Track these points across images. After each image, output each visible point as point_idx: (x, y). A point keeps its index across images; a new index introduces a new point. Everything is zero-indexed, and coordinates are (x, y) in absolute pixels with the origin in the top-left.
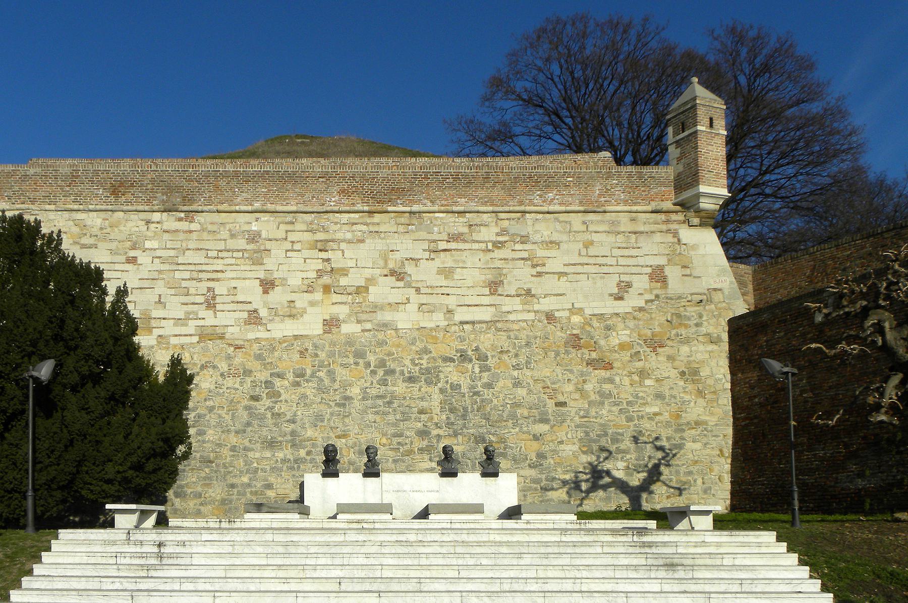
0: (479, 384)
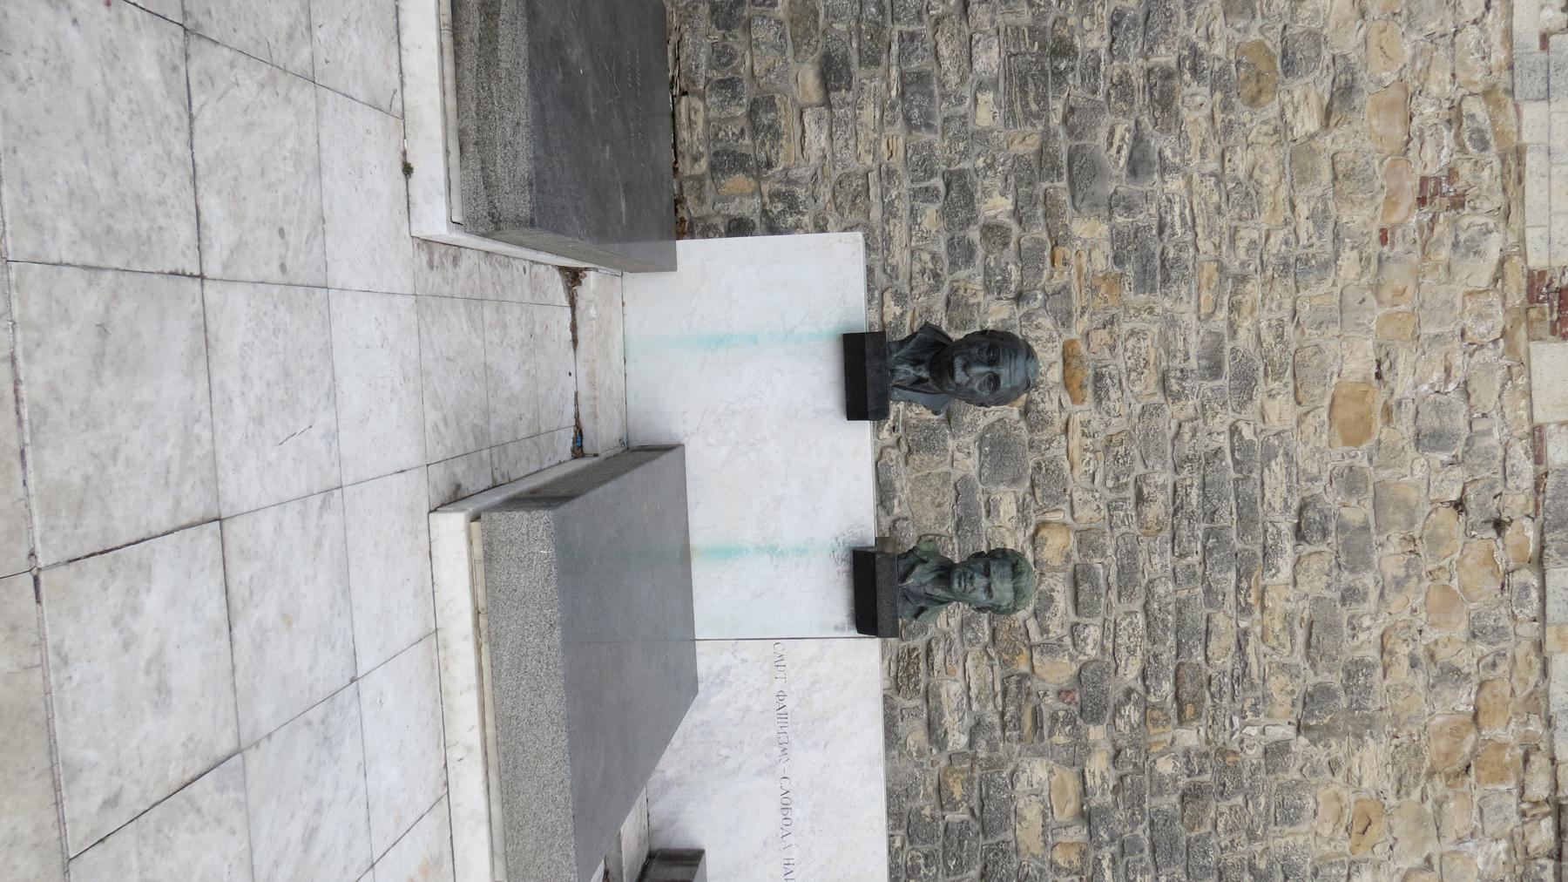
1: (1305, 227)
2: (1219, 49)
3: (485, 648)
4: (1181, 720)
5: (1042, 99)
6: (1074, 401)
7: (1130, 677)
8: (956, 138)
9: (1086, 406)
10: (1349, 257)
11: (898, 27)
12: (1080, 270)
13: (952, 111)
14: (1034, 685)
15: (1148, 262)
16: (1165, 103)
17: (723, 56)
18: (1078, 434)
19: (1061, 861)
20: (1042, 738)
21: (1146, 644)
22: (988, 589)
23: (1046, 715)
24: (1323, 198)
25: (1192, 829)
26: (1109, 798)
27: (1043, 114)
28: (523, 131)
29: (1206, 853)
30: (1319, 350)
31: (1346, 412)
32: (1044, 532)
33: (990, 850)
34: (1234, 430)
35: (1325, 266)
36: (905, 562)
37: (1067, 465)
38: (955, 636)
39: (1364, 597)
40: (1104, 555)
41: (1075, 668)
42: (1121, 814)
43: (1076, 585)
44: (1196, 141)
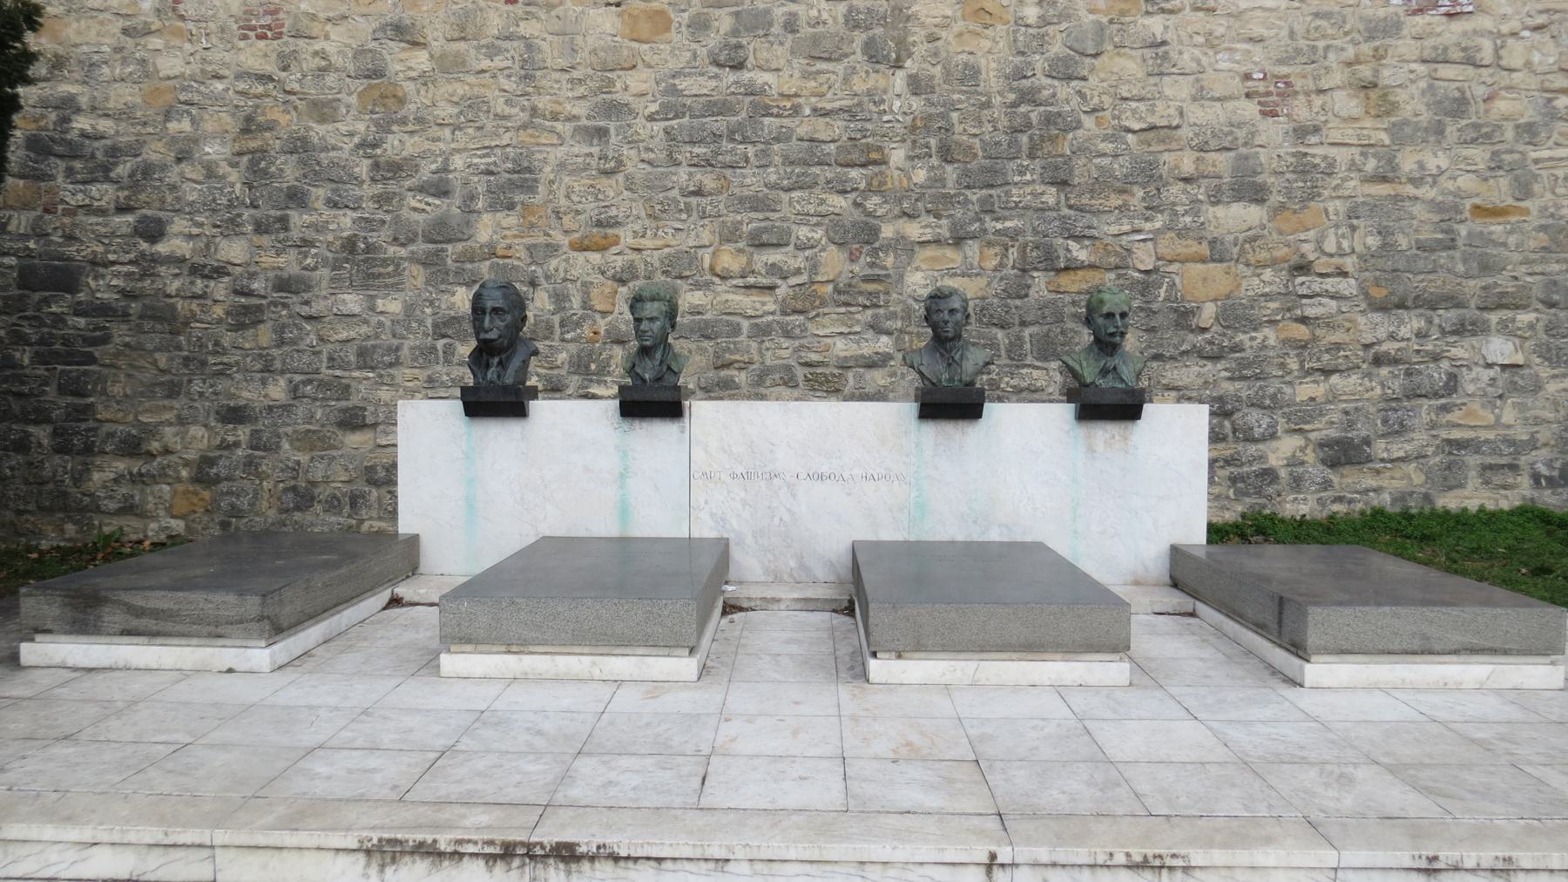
0: (1039, 62)
1: (499, 62)
2: (361, 127)
3: (532, 649)
4: (885, 163)
5: (385, 262)
6: (617, 244)
7: (844, 203)
8: (408, 329)
9: (621, 234)
10: (525, 29)
11: (323, 370)
12: (515, 236)
13: (388, 331)
14: (843, 280)
15: (515, 183)
16: (396, 169)
17: (333, 504)
18: (643, 241)
19: (994, 263)
20: (888, 276)
21: (817, 190)
22: (651, 319)
23: (870, 272)
24: (479, 48)
25: (976, 155)
26: (944, 222)
27: (396, 262)
28: (210, 597)
29: (998, 143)
30: (594, 52)
31: (645, 28)
32: (718, 270)
33: (980, 321)
34: (651, 118)
35: (529, 47)
37: (666, 250)
38: (797, 343)
39: (793, 15)
40: (741, 223)
41: (833, 247)
42: (958, 213)
43: (763, 245)
44: (427, 145)
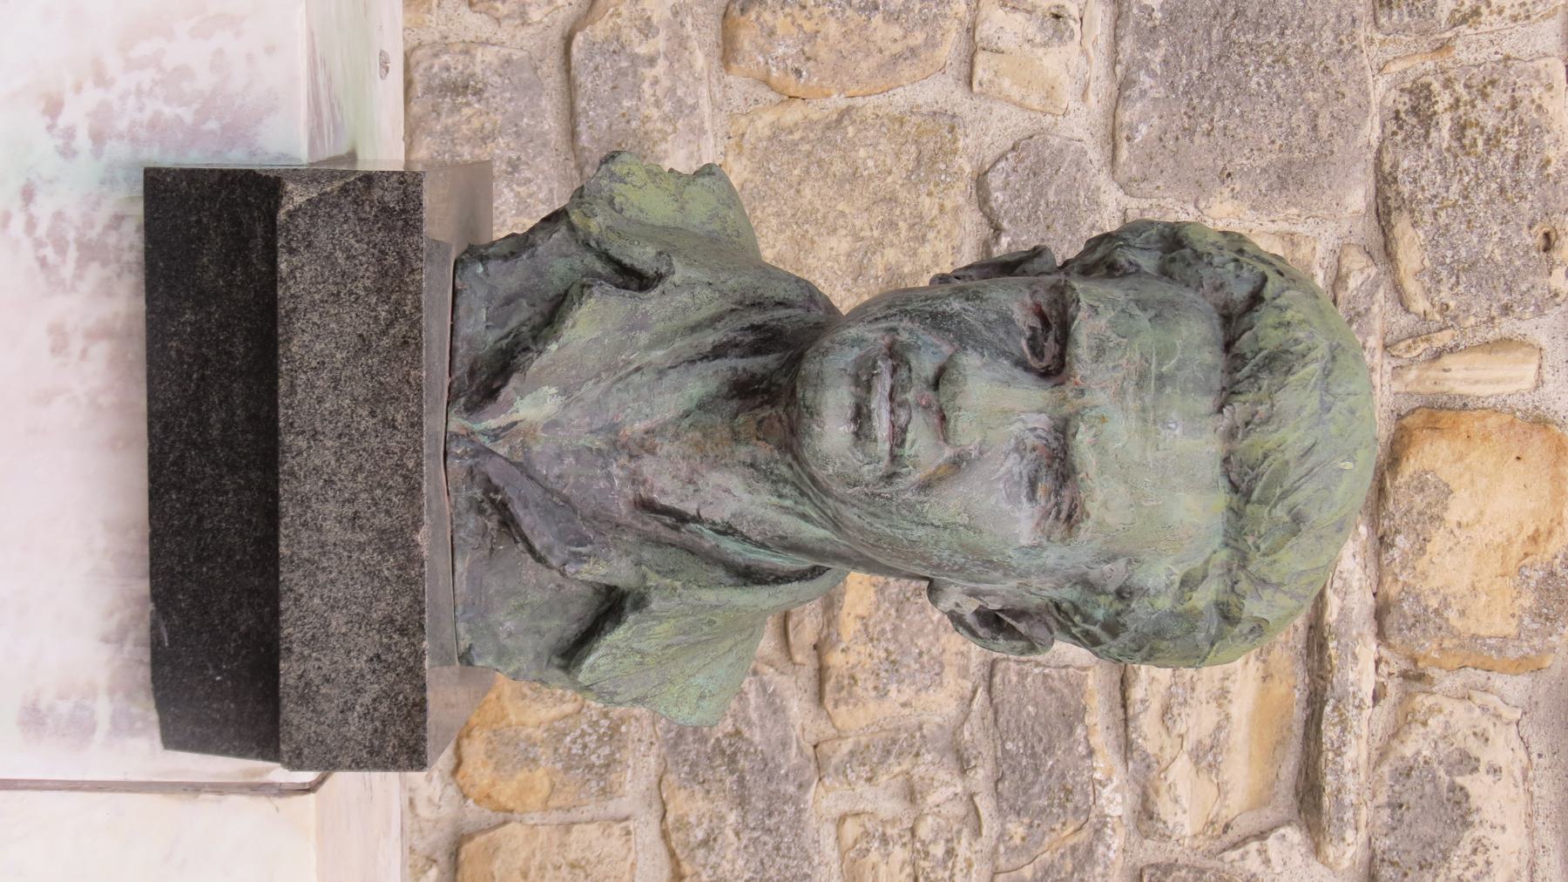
22: (1057, 465)
36: (509, 277)
